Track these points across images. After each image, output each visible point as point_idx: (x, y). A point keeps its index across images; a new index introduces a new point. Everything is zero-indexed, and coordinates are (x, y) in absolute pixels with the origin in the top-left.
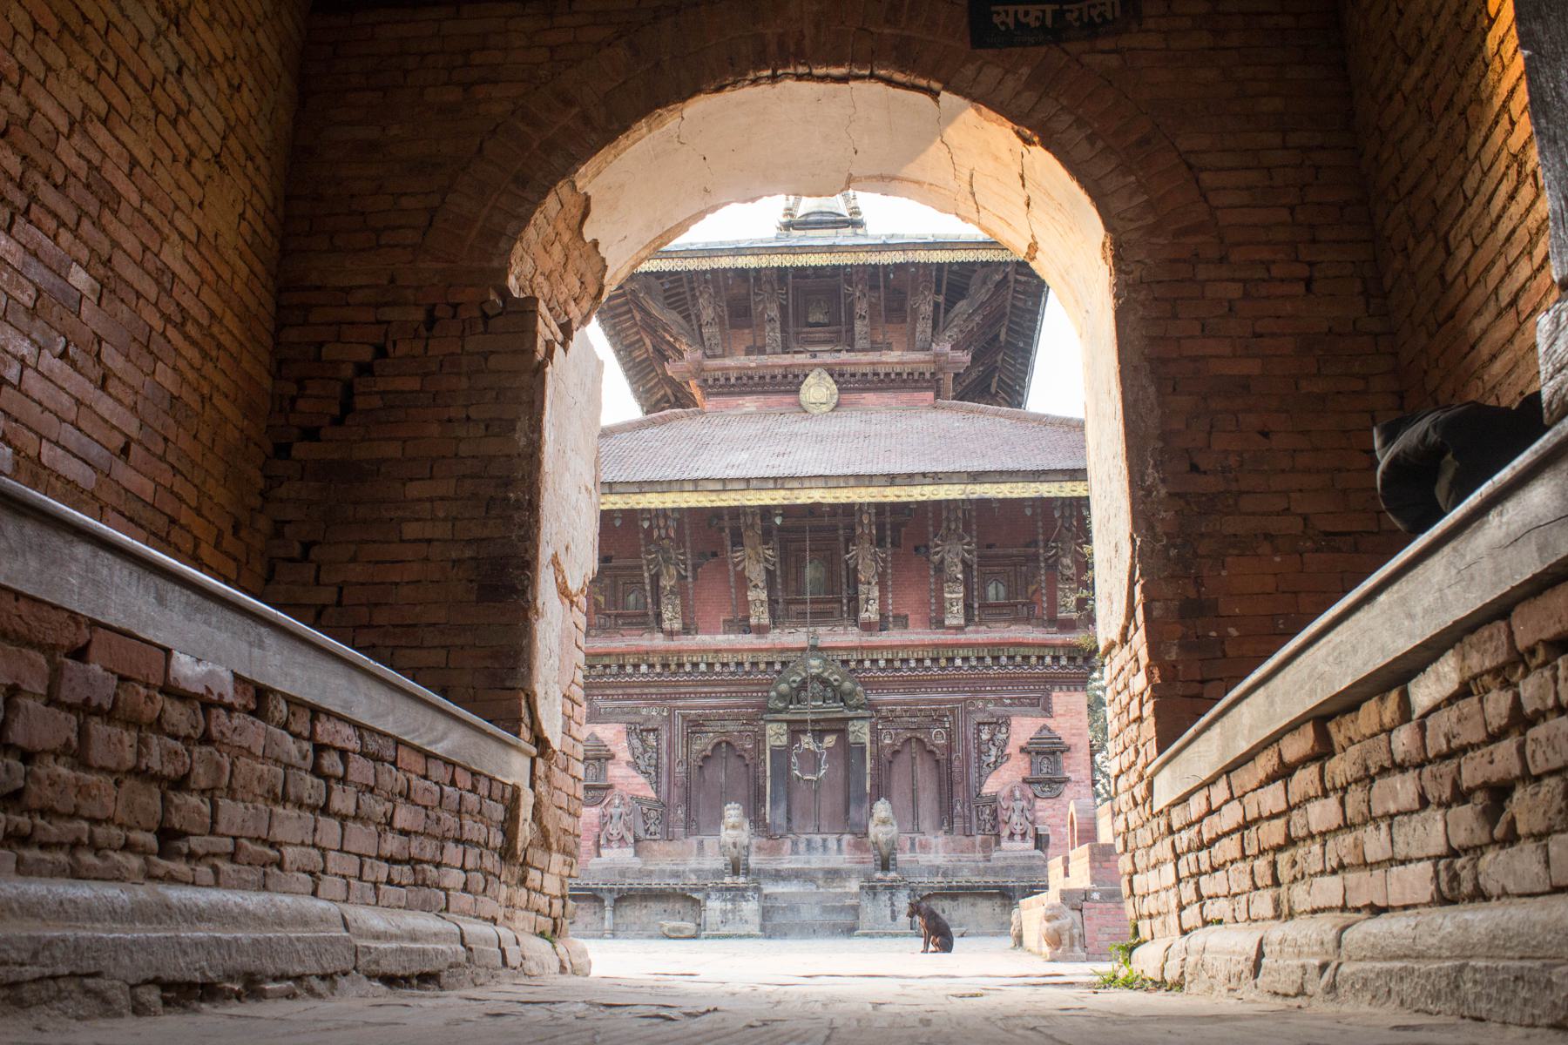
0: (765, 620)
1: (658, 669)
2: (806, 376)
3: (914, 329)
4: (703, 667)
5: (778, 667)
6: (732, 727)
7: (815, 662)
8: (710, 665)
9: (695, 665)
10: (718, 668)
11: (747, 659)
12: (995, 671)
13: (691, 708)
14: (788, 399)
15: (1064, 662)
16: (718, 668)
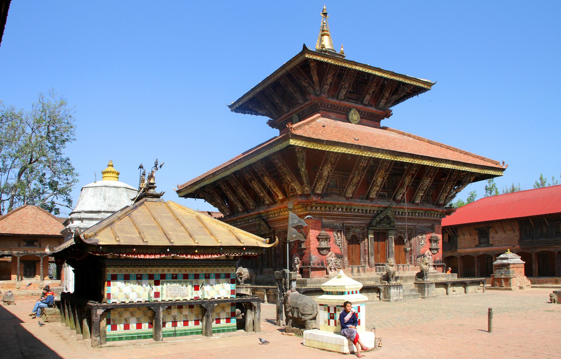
0: (374, 197)
1: (344, 210)
2: (350, 110)
3: (380, 101)
4: (356, 210)
5: (375, 212)
6: (358, 230)
7: (389, 212)
8: (358, 210)
9: (354, 209)
10: (360, 211)
11: (368, 209)
12: (423, 217)
13: (349, 223)
14: (343, 116)
15: (439, 216)
16: (360, 211)
